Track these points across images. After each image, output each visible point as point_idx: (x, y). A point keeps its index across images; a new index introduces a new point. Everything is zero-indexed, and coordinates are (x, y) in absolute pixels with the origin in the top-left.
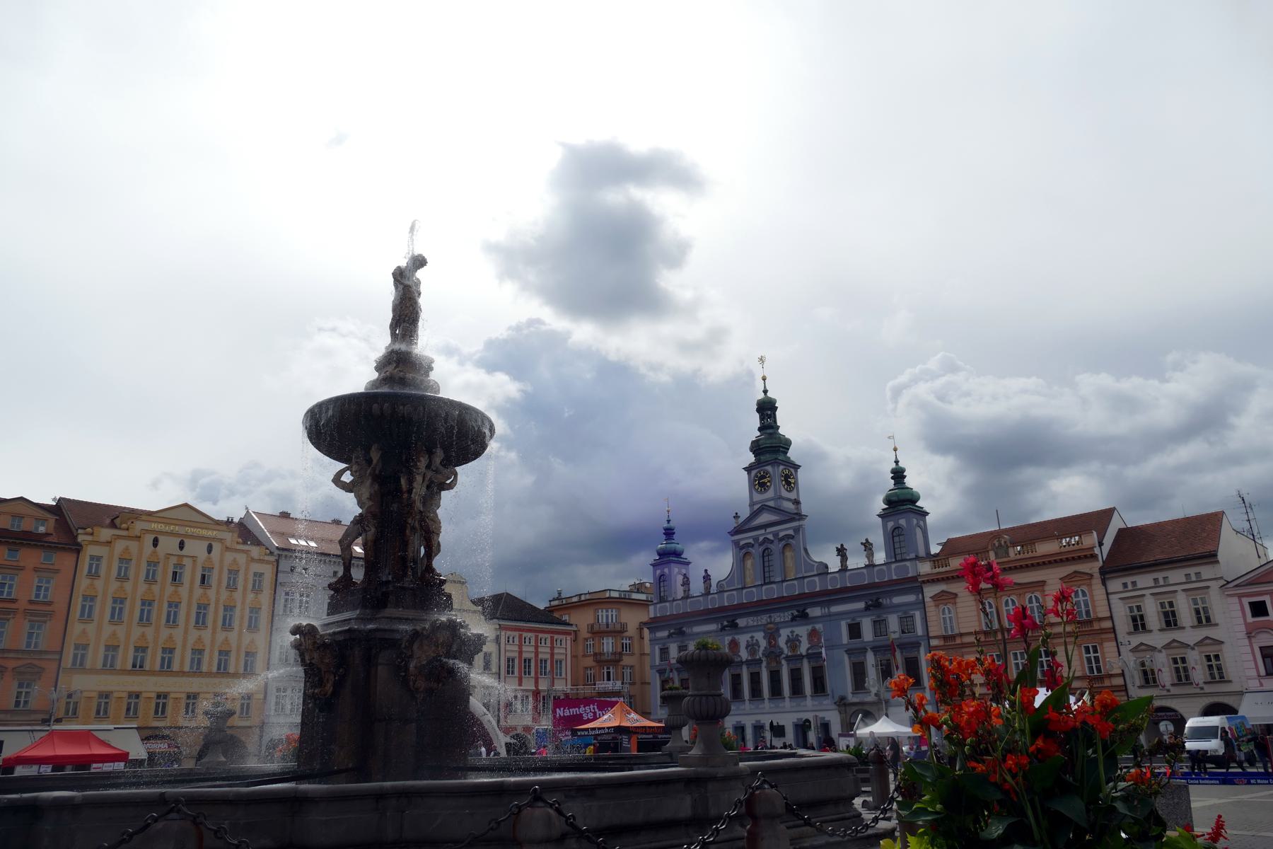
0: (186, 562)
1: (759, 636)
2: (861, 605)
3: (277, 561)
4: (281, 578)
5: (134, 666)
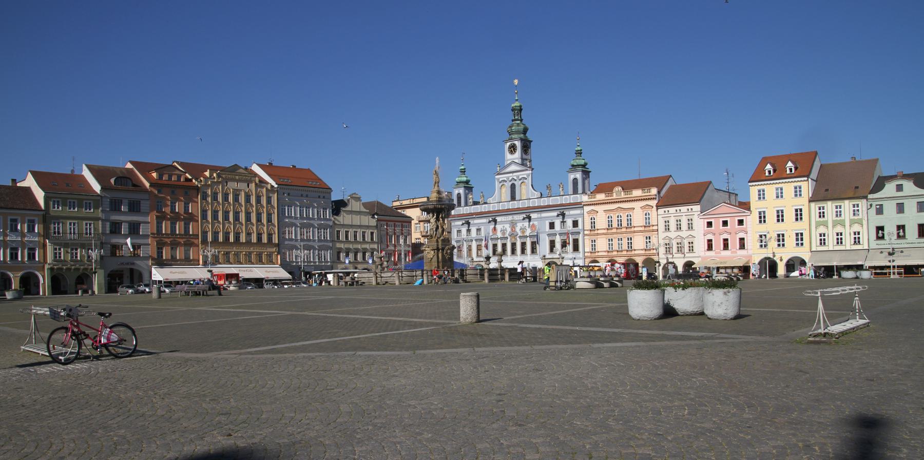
1: (508, 227)
2: (555, 214)
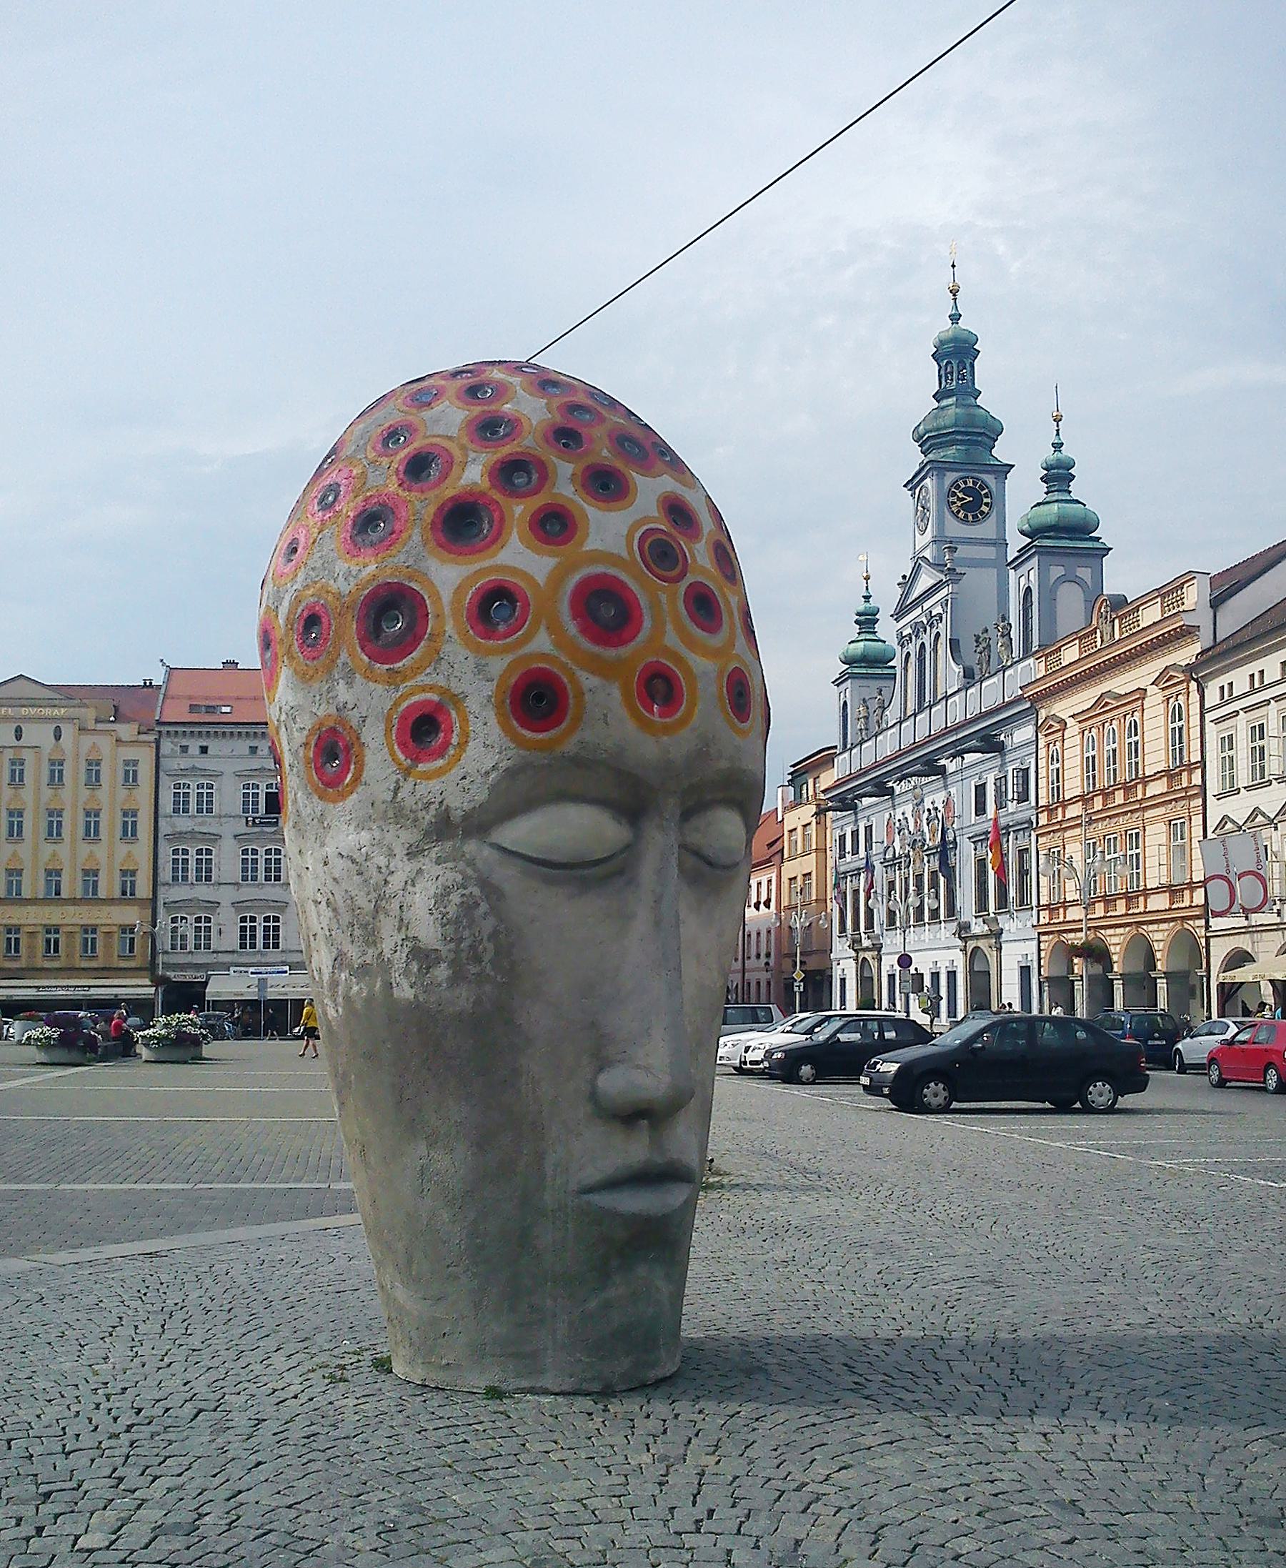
0: (28, 755)
3: (157, 742)
5: (124, 893)
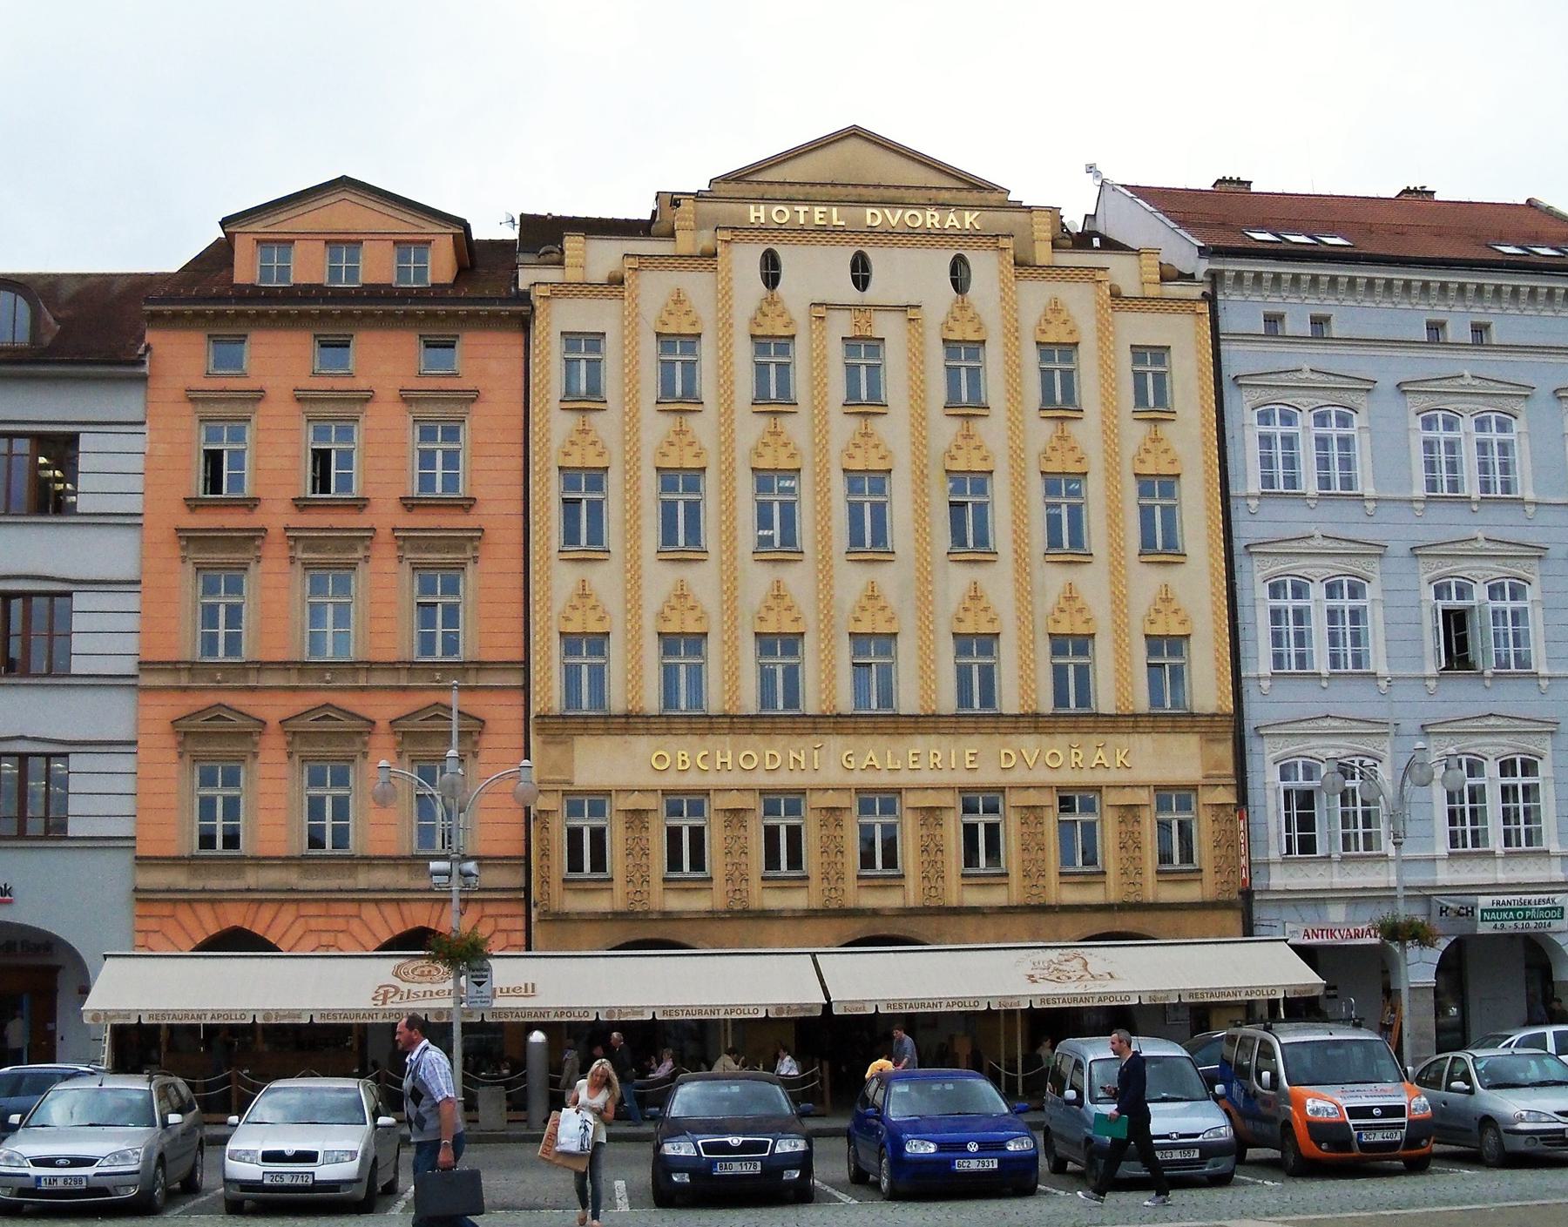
0: (888, 327)
3: (1210, 298)
4: (1237, 359)
